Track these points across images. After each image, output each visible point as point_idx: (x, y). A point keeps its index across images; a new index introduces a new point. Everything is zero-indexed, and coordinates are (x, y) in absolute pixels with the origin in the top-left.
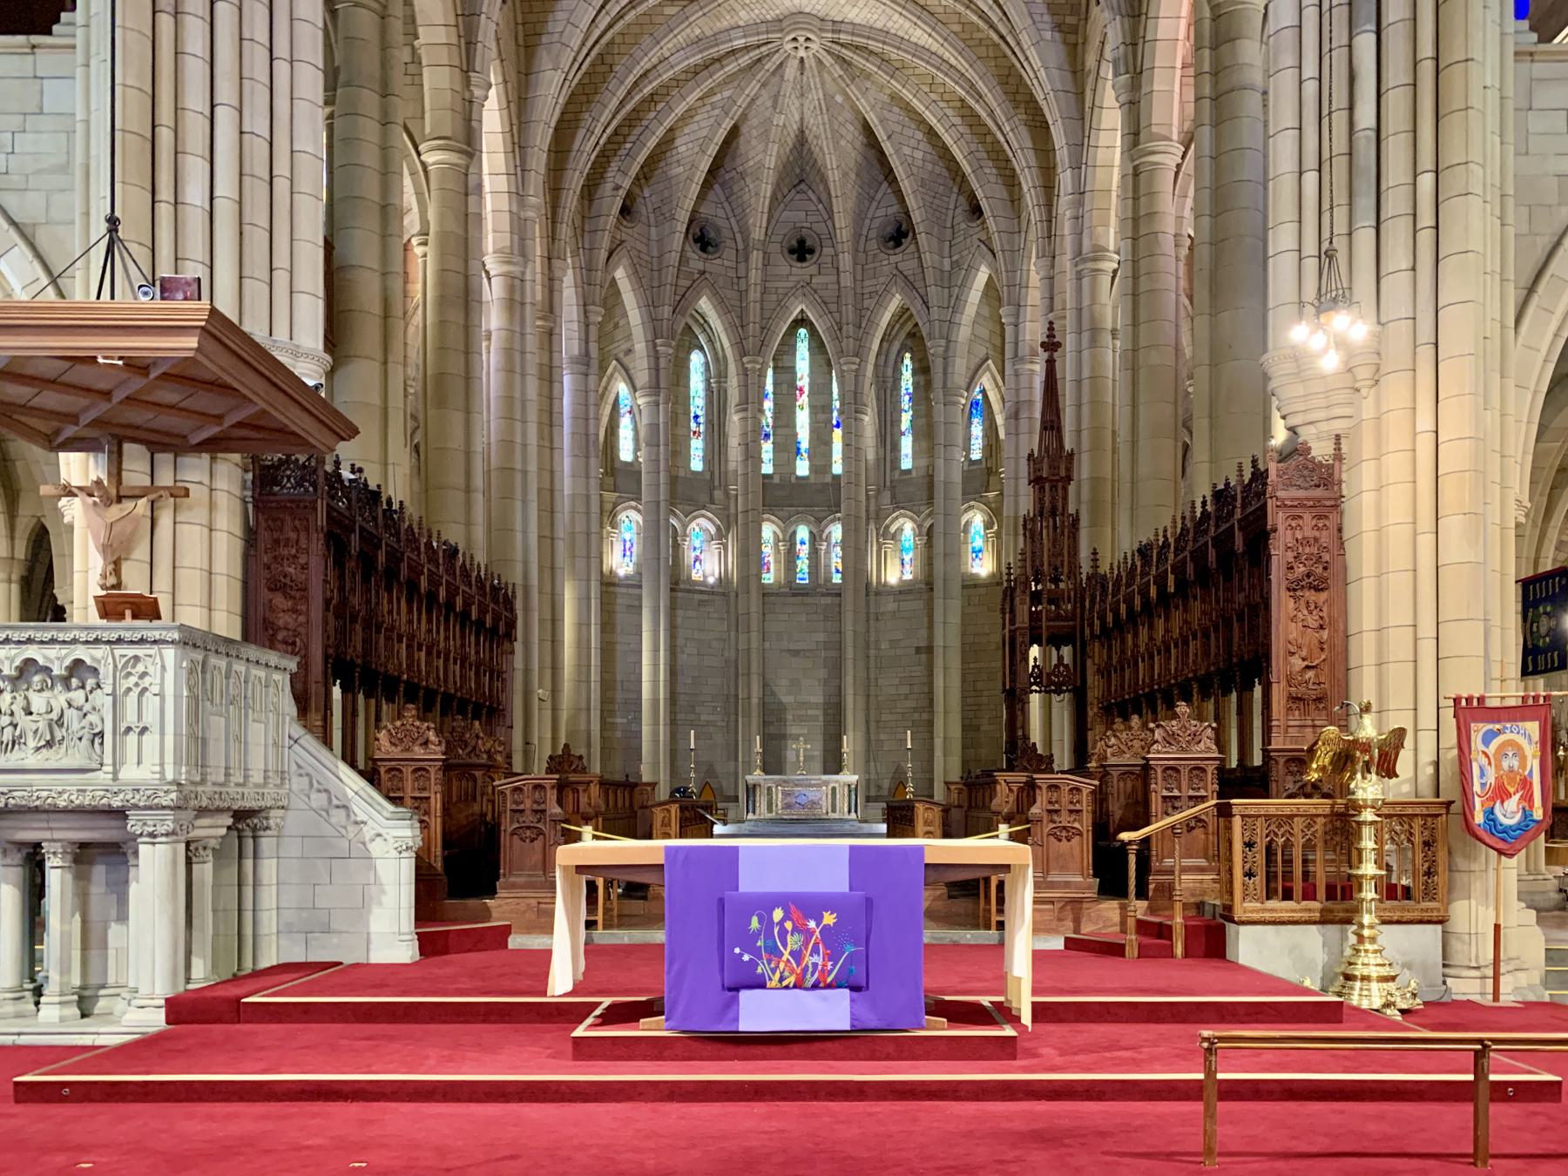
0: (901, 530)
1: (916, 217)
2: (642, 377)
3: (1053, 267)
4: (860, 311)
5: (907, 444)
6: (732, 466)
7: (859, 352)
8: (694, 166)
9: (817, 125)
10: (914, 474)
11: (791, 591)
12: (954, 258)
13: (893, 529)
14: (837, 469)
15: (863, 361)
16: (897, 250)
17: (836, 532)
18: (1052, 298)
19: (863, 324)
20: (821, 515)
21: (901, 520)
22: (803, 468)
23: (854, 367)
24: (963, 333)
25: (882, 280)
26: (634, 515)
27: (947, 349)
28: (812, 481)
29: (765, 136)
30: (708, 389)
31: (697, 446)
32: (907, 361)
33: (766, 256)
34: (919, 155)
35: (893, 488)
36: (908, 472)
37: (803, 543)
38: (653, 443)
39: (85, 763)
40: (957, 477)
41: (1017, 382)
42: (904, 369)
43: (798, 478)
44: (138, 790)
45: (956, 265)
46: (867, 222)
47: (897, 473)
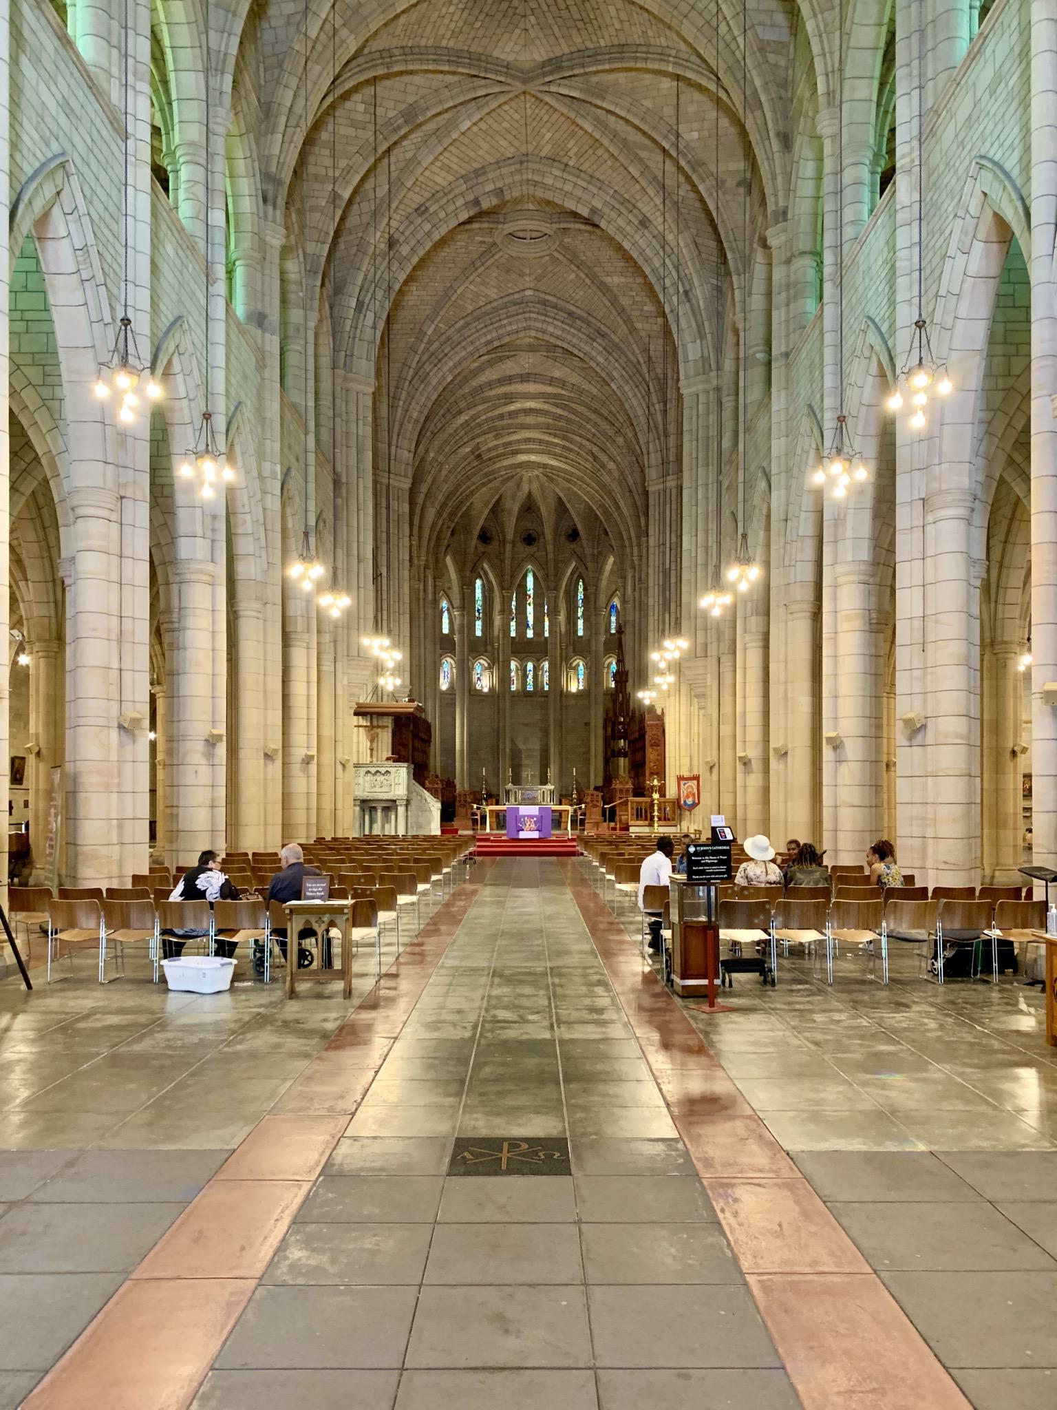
1: (581, 533)
2: (457, 603)
4: (557, 569)
5: (580, 623)
6: (496, 633)
7: (556, 588)
8: (481, 513)
9: (537, 495)
11: (524, 694)
14: (547, 634)
17: (546, 665)
19: (558, 574)
22: (530, 634)
24: (604, 583)
26: (449, 660)
29: (514, 497)
30: (484, 596)
31: (479, 624)
33: (514, 543)
38: (461, 632)
40: (601, 648)
45: (600, 553)
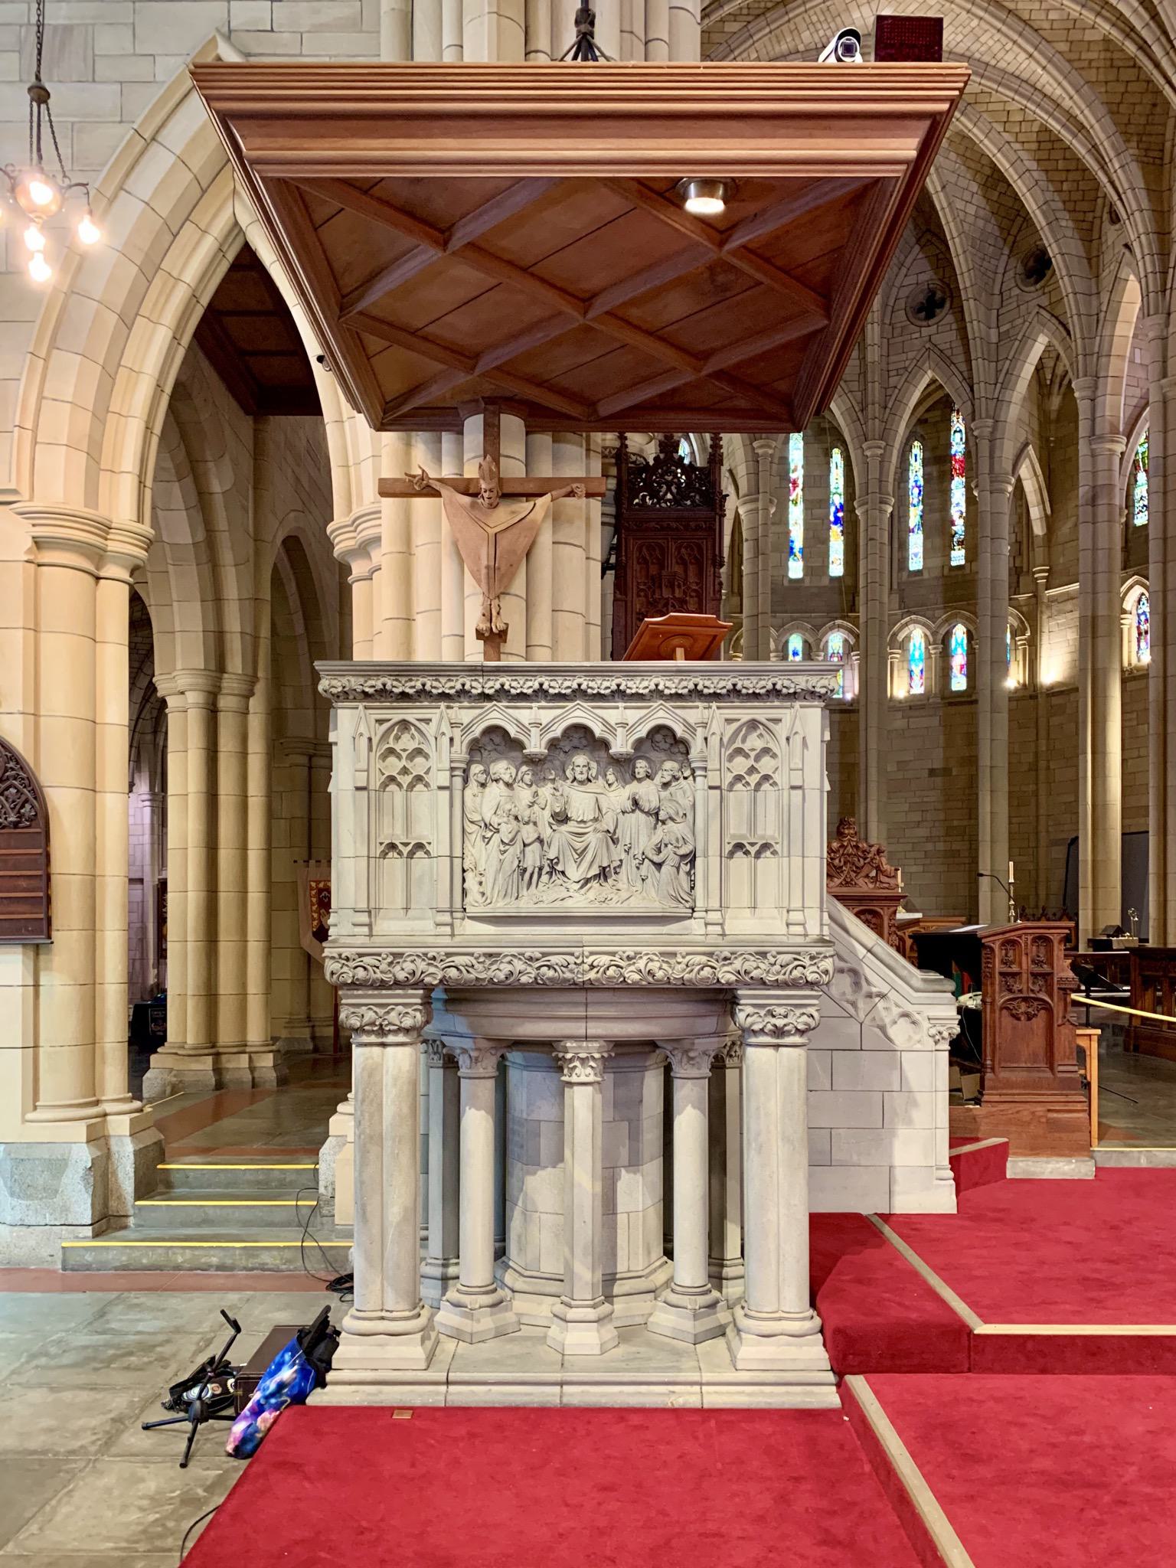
0: (908, 638)
3: (1167, 325)
10: (926, 575)
12: (1003, 329)
13: (901, 637)
15: (889, 445)
16: (931, 322)
18: (1165, 362)
20: (819, 621)
21: (911, 627)
23: (880, 452)
25: (911, 355)
27: (995, 428)
28: (807, 583)
32: (917, 449)
34: (971, 209)
35: (901, 591)
36: (918, 573)
37: (795, 654)
39: (670, 907)
41: (1094, 464)
42: (912, 460)
43: (792, 581)
44: (764, 955)
46: (895, 290)
47: (905, 574)
